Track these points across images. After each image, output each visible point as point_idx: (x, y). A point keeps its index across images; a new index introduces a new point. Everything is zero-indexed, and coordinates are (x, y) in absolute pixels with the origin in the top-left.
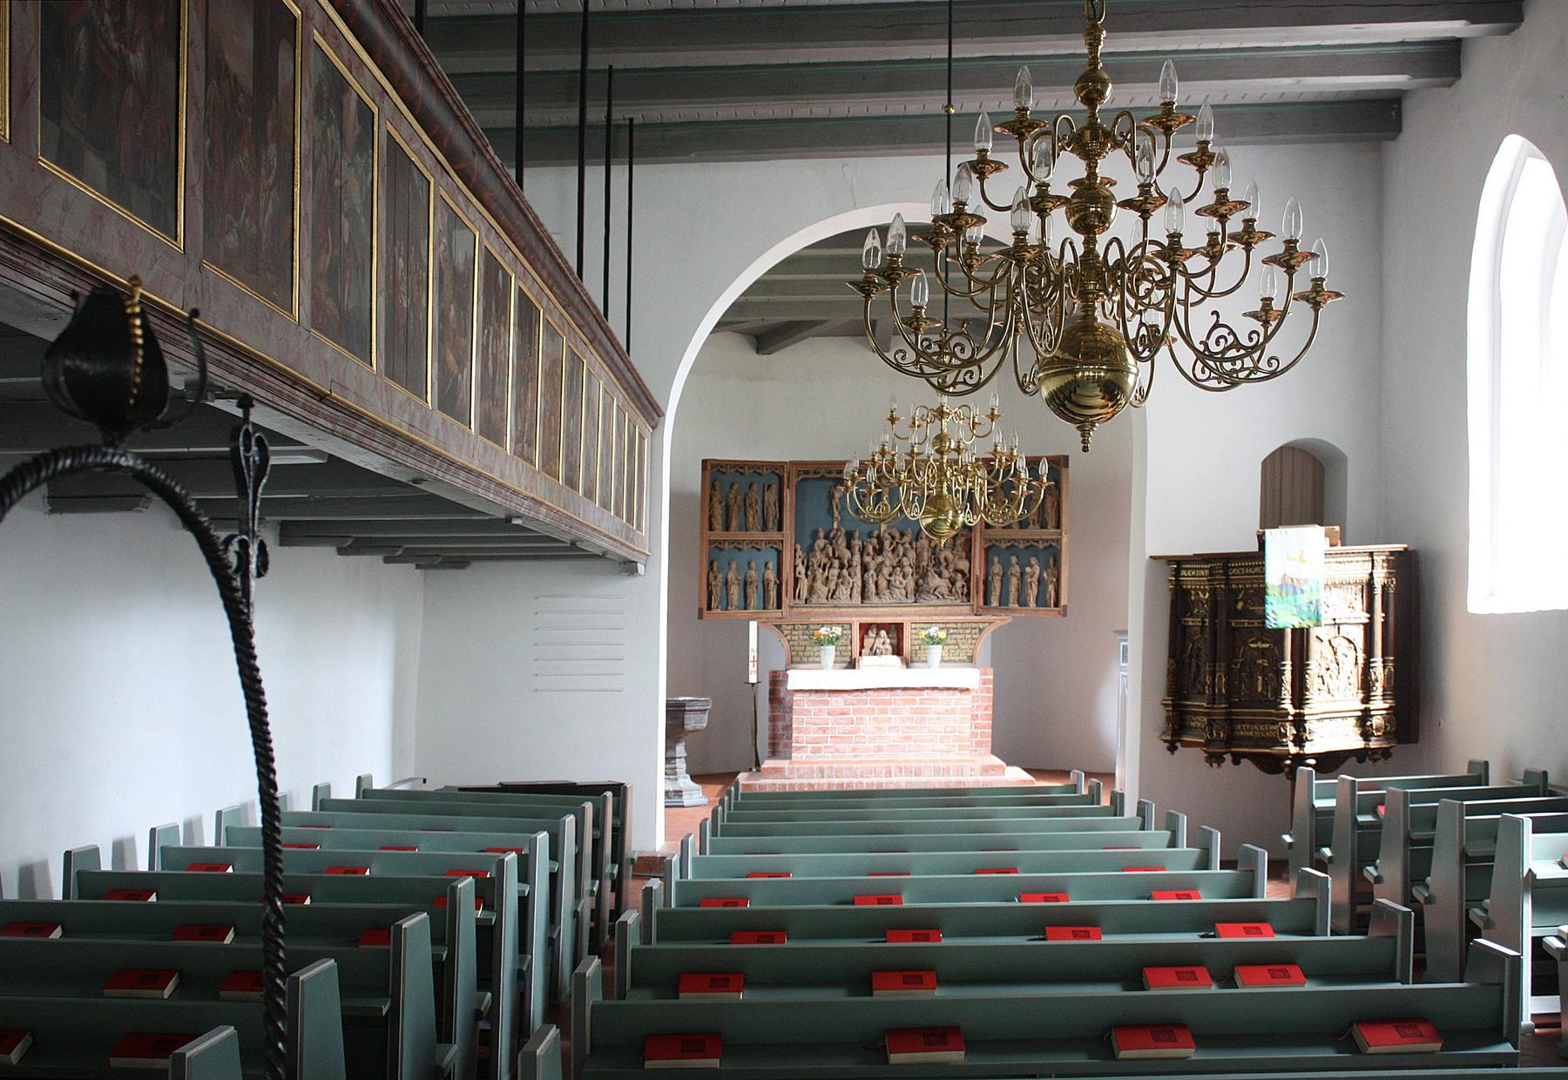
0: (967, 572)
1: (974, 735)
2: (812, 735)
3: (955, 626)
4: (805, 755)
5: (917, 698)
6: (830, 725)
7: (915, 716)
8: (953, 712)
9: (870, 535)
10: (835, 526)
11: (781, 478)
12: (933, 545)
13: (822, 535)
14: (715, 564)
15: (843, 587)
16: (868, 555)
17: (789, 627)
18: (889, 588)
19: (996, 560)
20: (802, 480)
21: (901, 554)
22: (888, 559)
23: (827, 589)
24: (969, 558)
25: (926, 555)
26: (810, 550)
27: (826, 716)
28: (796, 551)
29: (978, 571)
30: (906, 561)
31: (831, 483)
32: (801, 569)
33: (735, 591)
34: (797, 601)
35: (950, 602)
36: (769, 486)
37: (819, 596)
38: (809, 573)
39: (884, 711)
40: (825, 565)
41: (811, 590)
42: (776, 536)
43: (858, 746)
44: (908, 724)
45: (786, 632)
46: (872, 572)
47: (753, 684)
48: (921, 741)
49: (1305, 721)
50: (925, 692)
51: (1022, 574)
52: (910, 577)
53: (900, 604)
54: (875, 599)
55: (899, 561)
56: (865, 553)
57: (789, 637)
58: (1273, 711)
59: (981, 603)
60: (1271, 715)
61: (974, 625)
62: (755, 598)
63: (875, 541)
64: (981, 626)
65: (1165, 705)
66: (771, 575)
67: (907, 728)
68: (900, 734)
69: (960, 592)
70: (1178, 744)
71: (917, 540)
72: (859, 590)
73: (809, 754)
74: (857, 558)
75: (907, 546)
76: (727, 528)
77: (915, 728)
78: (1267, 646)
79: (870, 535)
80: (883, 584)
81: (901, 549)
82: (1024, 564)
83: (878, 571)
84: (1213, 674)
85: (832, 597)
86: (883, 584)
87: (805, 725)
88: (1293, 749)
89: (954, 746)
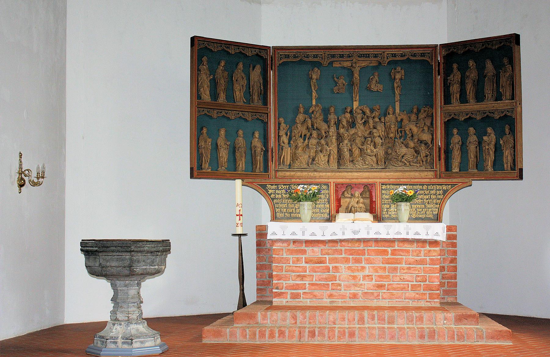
1: (442, 285)
2: (291, 282)
4: (285, 300)
5: (389, 249)
6: (308, 273)
7: (387, 266)
8: (422, 262)
9: (344, 111)
10: (314, 103)
13: (302, 110)
15: (321, 155)
17: (273, 187)
18: (361, 156)
19: (455, 131)
21: (372, 127)
22: (360, 130)
23: (306, 157)
26: (292, 123)
27: (304, 264)
29: (439, 142)
30: (376, 133)
32: (285, 139)
35: (416, 169)
37: (301, 162)
39: (358, 261)
40: (305, 135)
41: (294, 157)
44: (381, 273)
45: (270, 191)
46: (346, 142)
48: (395, 289)
53: (371, 169)
55: (370, 133)
57: (272, 196)
61: (438, 187)
63: (348, 115)
64: (445, 188)
68: (374, 282)
71: (385, 115)
72: (335, 157)
73: (289, 299)
74: (333, 130)
80: (356, 152)
81: (371, 121)
82: (481, 134)
83: (352, 140)
85: (311, 164)
86: (356, 152)
87: (284, 273)
89: (425, 294)
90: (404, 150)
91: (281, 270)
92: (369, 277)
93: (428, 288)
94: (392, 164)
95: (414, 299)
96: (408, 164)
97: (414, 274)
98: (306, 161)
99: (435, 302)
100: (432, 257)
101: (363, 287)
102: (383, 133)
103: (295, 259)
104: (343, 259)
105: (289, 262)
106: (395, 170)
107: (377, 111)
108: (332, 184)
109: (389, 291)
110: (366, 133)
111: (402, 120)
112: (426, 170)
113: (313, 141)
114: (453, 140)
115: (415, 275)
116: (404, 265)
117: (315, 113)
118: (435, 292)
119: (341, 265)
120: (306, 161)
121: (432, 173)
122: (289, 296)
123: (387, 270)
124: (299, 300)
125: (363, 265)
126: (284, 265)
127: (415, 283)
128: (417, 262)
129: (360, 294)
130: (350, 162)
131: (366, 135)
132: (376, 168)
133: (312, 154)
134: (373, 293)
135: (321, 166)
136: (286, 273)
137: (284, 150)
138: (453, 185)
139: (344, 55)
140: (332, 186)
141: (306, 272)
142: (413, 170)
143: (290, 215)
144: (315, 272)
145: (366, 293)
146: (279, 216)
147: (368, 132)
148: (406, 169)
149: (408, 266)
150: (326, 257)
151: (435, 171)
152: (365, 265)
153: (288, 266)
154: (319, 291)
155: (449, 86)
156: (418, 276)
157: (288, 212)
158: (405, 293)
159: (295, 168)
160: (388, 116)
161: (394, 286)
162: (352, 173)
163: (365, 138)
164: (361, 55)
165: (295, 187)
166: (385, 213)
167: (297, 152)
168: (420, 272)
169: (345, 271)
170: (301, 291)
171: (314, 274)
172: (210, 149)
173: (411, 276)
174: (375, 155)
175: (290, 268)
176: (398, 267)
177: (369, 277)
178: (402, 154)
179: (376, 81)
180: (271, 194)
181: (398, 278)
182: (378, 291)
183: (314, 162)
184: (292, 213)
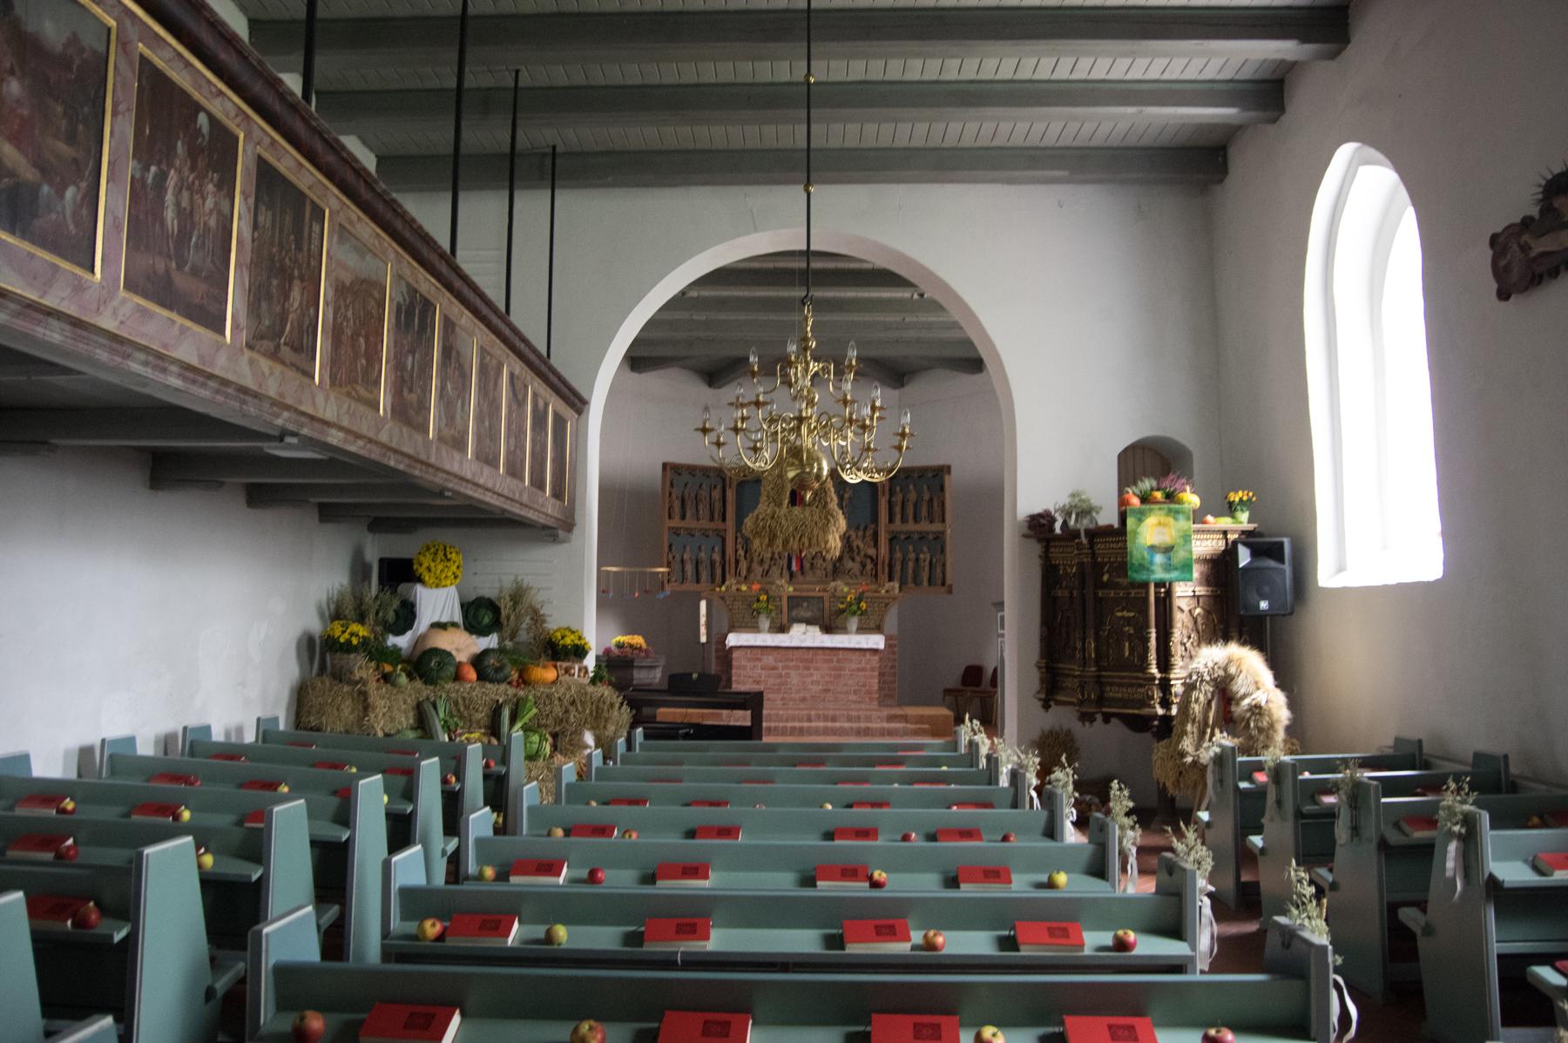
0: (874, 557)
1: (880, 689)
5: (835, 659)
7: (833, 673)
8: (863, 670)
11: (724, 480)
14: (674, 548)
24: (876, 545)
28: (736, 538)
32: (741, 552)
33: (689, 568)
39: (808, 669)
41: (749, 570)
42: (720, 526)
44: (827, 679)
47: (703, 644)
48: (840, 693)
49: (1172, 685)
50: (841, 652)
51: (917, 559)
58: (1140, 675)
60: (1137, 678)
62: (704, 575)
65: (1040, 668)
66: (717, 557)
67: (827, 682)
68: (820, 687)
70: (1052, 703)
76: (683, 517)
78: (1132, 614)
82: (918, 552)
84: (1084, 640)
88: (1160, 711)
91: (740, 676)
92: (818, 683)
93: (868, 692)
95: (855, 702)
111: (849, 537)
125: (812, 671)
128: (859, 670)
148: (851, 581)
177: (818, 683)
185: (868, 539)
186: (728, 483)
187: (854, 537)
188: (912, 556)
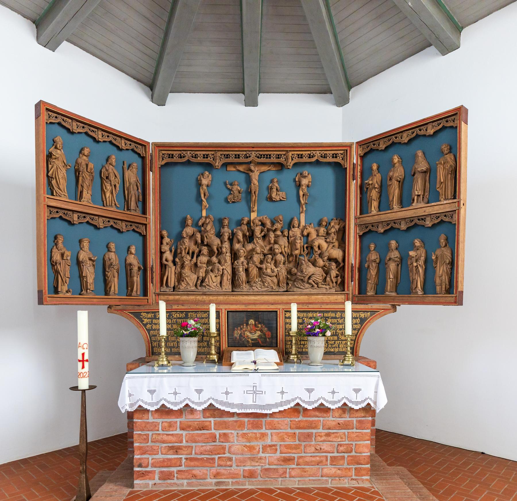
0: (340, 260)
2: (160, 456)
3: (333, 315)
4: (151, 482)
6: (184, 443)
7: (297, 431)
10: (204, 214)
12: (305, 233)
13: (189, 222)
15: (211, 274)
16: (239, 242)
17: (150, 316)
18: (260, 276)
20: (167, 164)
21: (272, 242)
22: (259, 245)
23: (195, 277)
25: (299, 243)
27: (178, 432)
28: (162, 237)
29: (353, 258)
31: (198, 170)
32: (168, 256)
34: (164, 288)
35: (324, 291)
36: (129, 166)
38: (177, 260)
40: (193, 253)
43: (222, 470)
44: (289, 442)
45: (146, 321)
46: (242, 259)
48: (307, 463)
52: (281, 265)
53: (272, 292)
54: (245, 287)
55: (271, 249)
56: (235, 240)
57: (149, 326)
59: (357, 293)
63: (245, 228)
66: (134, 260)
67: (288, 447)
68: (278, 454)
69: (334, 280)
71: (289, 229)
72: (229, 277)
73: (157, 481)
75: (279, 233)
77: (297, 447)
79: (239, 223)
80: (254, 271)
81: (272, 235)
83: (249, 257)
86: (254, 271)
87: (150, 444)
90: (310, 269)
92: (272, 447)
93: (356, 461)
94: (297, 286)
95: (333, 476)
96: (316, 285)
97: (334, 443)
98: (193, 282)
99: (363, 480)
100: (360, 419)
101: (263, 461)
102: (286, 249)
103: (166, 424)
104: (235, 424)
105: (157, 428)
106: (300, 293)
107: (280, 222)
108: (223, 311)
109: (299, 467)
110: (265, 249)
111: (308, 235)
112: (337, 292)
113: (204, 259)
114: (369, 257)
115: (336, 444)
116: (321, 430)
117: (205, 225)
118: (363, 466)
119: (233, 432)
120: (193, 282)
121: (343, 297)
122: (157, 477)
123: (297, 437)
124: (172, 481)
125: (263, 431)
126: (150, 433)
127: (336, 454)
128: (339, 426)
129: (259, 471)
130: (246, 284)
131: (266, 252)
132: (277, 290)
133: (201, 275)
134: (277, 469)
135: (211, 288)
136: (153, 444)
137: (167, 269)
138: (373, 312)
139: (241, 155)
140: (223, 314)
141: (181, 442)
142: (321, 293)
143: (171, 350)
144: (196, 442)
145: (267, 470)
146: (156, 351)
147: (268, 248)
149: (326, 431)
150: (210, 421)
151: (346, 293)
152: (267, 431)
153: (156, 434)
154: (200, 469)
155: (366, 192)
156: (341, 445)
157: (168, 346)
158: (322, 469)
159: (181, 290)
160: (293, 229)
161: (308, 459)
162: (248, 297)
163: (265, 255)
164: (261, 155)
165: (177, 315)
166: (289, 347)
167: (183, 271)
168: (344, 440)
169: (237, 440)
170: (175, 469)
171: (194, 445)
172: (69, 266)
173: (331, 445)
174: (276, 275)
175: (159, 438)
176: (312, 433)
178: (310, 275)
179: (277, 189)
180: (147, 324)
181: (313, 449)
182: (284, 467)
183: (204, 284)
184: (174, 347)
185: (333, 237)
186: (148, 162)
187: (314, 235)
188: (395, 255)
